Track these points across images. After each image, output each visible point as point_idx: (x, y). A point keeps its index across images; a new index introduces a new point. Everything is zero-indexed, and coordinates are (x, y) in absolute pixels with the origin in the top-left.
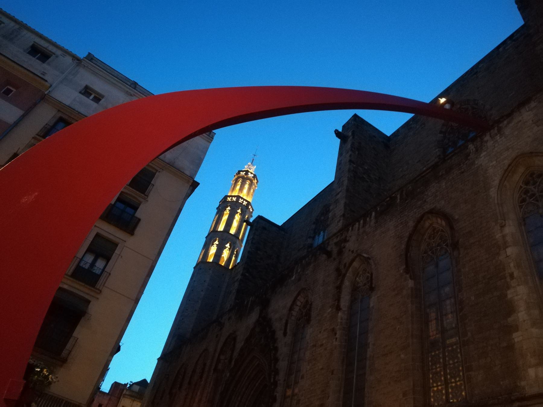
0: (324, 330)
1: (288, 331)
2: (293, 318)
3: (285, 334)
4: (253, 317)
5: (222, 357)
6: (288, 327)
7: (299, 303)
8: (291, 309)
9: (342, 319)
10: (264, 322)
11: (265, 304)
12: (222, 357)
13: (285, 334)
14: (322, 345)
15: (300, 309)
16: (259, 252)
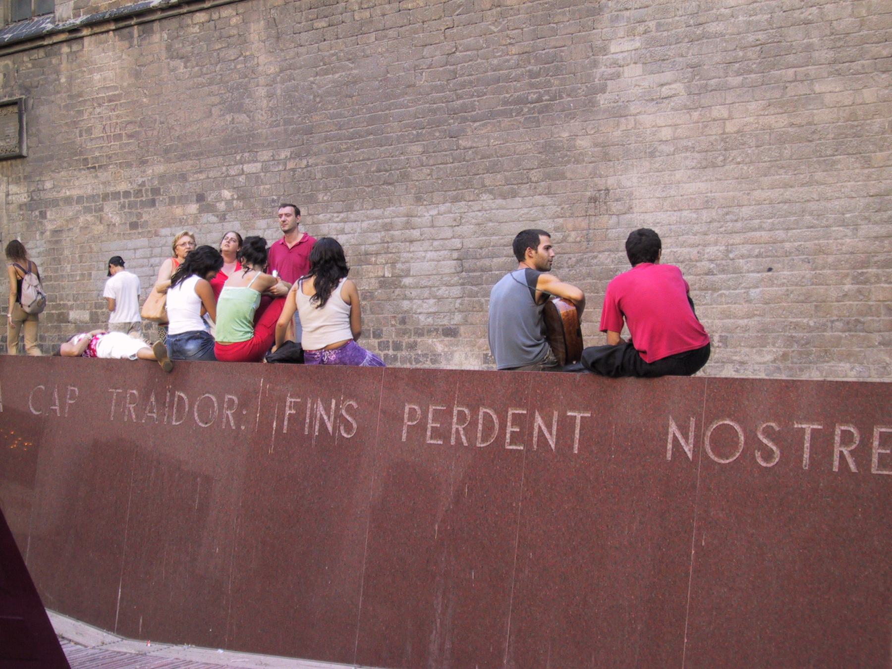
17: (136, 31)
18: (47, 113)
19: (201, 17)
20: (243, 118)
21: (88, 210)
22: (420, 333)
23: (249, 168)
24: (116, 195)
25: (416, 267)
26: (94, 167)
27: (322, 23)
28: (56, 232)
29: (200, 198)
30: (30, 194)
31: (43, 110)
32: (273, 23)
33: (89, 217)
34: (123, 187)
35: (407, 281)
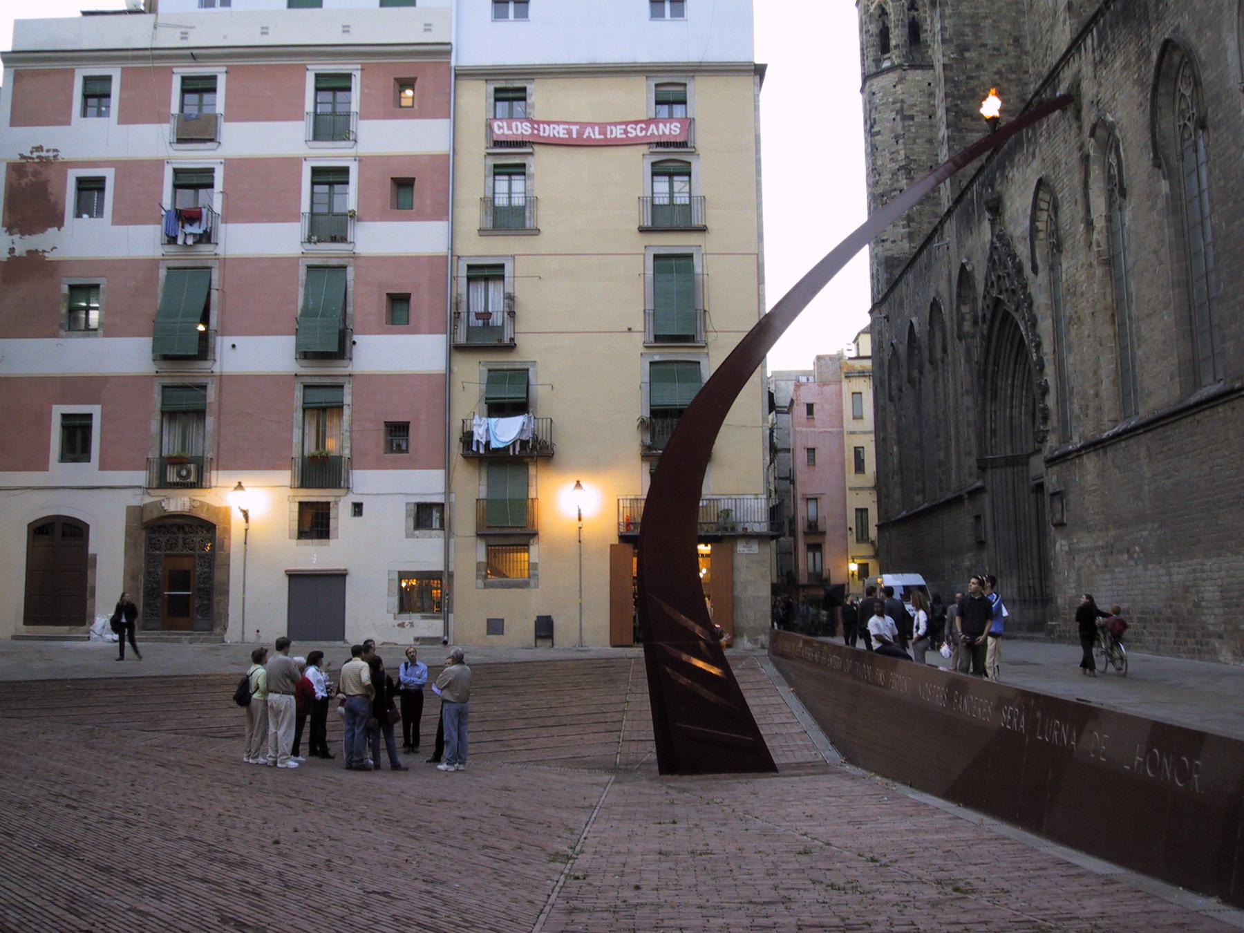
0: (1082, 265)
1: (1038, 262)
2: (1042, 235)
3: (1035, 269)
4: (985, 232)
5: (965, 309)
6: (1038, 255)
7: (1043, 205)
8: (1034, 219)
9: (1099, 245)
10: (1002, 242)
11: (996, 208)
12: (965, 309)
13: (1035, 269)
14: (1082, 294)
15: (1049, 216)
16: (967, 55)
17: (1101, 452)
18: (1072, 497)
19: (1123, 444)
20: (1140, 504)
21: (1089, 556)
22: (1211, 635)
23: (1145, 533)
24: (1097, 548)
25: (1207, 595)
26: (1089, 530)
27: (1165, 449)
28: (1079, 569)
29: (1128, 551)
30: (1070, 544)
31: (1071, 497)
32: (1148, 448)
33: (1089, 561)
34: (1101, 543)
35: (1203, 604)
